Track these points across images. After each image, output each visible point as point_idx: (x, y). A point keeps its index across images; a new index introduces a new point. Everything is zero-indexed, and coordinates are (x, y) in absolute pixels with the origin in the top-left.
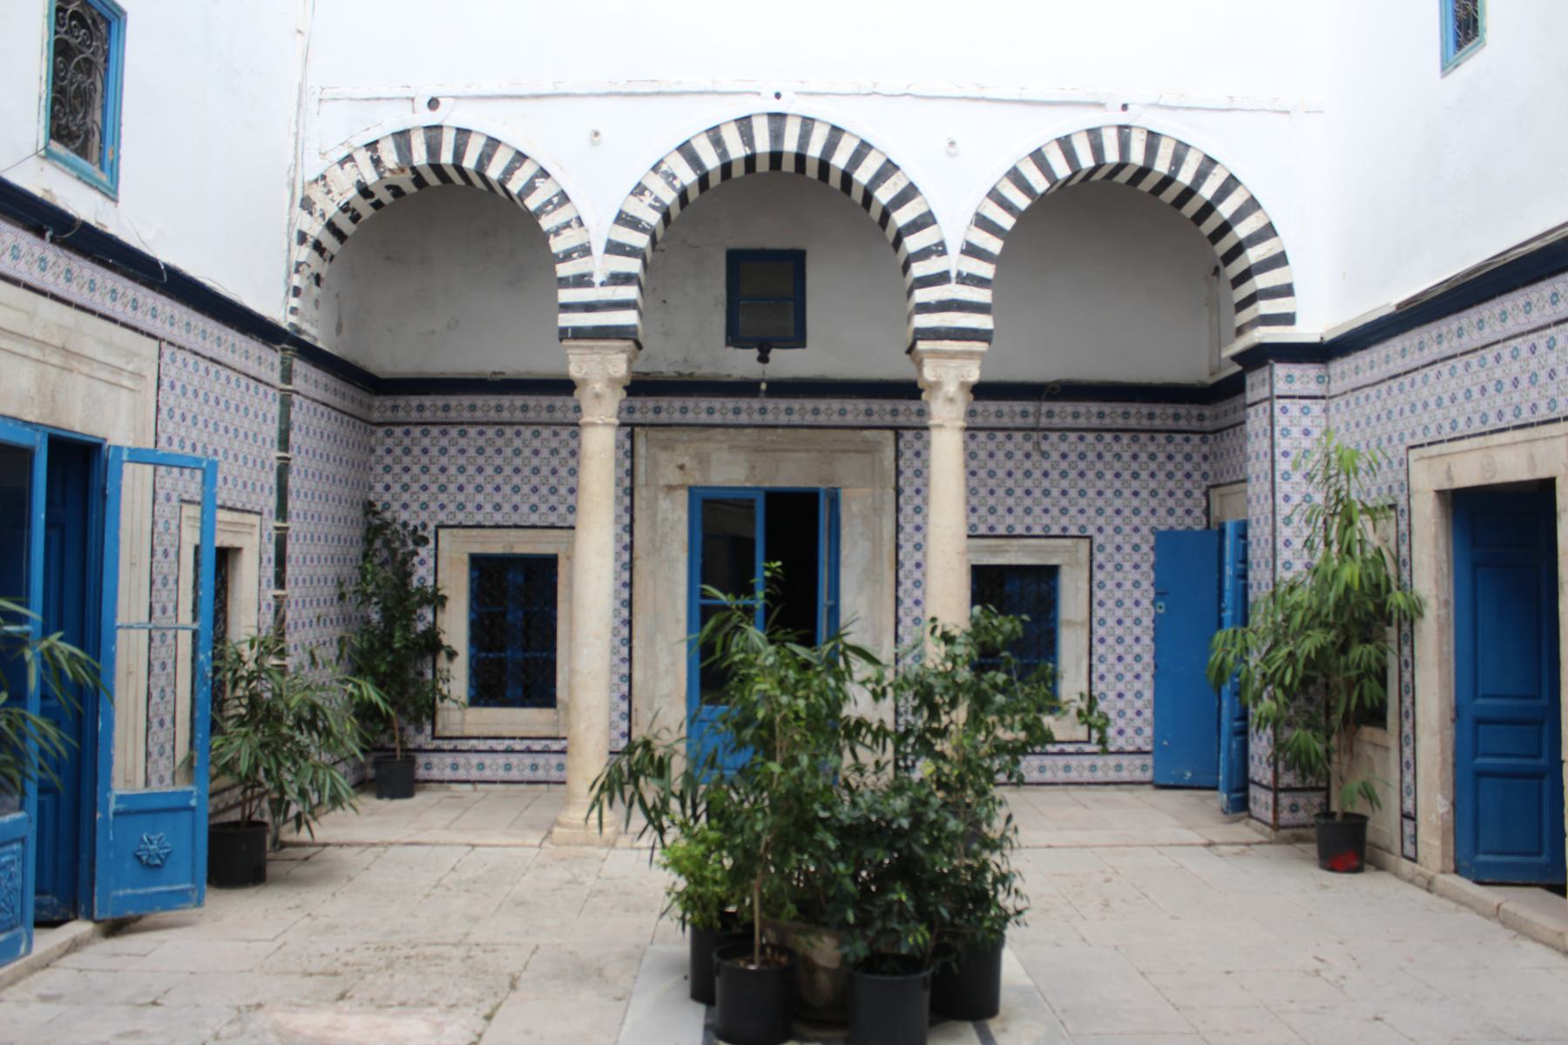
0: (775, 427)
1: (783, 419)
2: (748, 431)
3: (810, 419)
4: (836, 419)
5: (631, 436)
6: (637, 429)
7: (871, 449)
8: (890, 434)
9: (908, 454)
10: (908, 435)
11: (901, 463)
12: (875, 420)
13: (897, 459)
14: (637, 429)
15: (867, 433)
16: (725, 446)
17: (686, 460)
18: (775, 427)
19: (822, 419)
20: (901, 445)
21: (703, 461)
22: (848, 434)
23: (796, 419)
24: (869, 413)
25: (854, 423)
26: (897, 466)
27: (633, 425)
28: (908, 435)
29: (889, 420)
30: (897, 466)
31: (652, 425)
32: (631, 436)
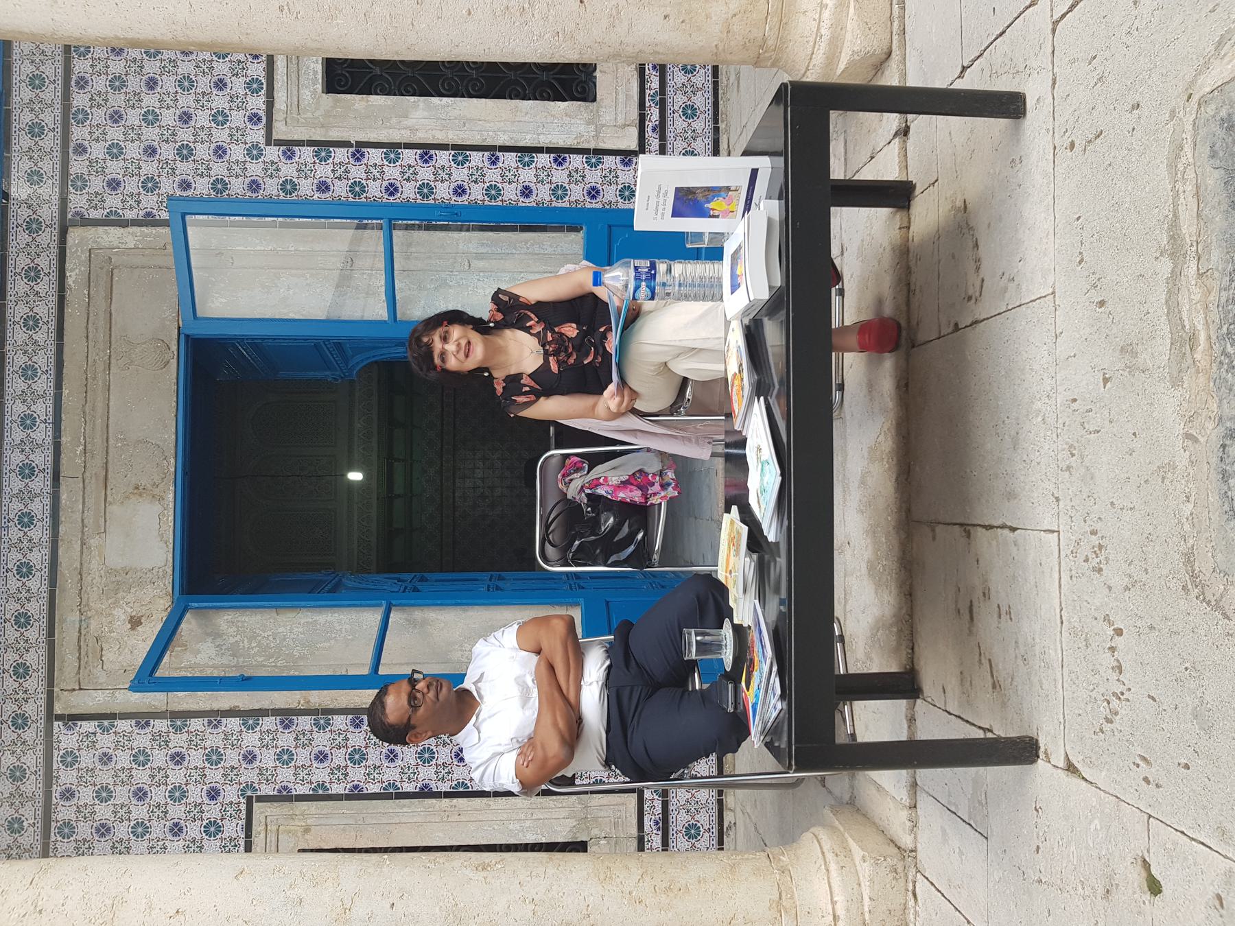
0: (57, 447)
1: (43, 433)
2: (64, 497)
3: (44, 384)
4: (45, 335)
5: (72, 719)
6: (58, 709)
7: (105, 271)
8: (74, 235)
9: (113, 201)
10: (78, 201)
11: (129, 215)
12: (46, 262)
13: (124, 223)
14: (58, 709)
15: (72, 278)
16: (94, 542)
17: (121, 615)
18: (57, 447)
19: (44, 360)
20: (95, 214)
21: (122, 581)
22: (74, 312)
23: (43, 409)
24: (33, 274)
25: (53, 299)
26: (135, 223)
27: (51, 716)
28: (78, 201)
29: (48, 238)
30: (135, 223)
31: (51, 681)
32: (72, 719)
